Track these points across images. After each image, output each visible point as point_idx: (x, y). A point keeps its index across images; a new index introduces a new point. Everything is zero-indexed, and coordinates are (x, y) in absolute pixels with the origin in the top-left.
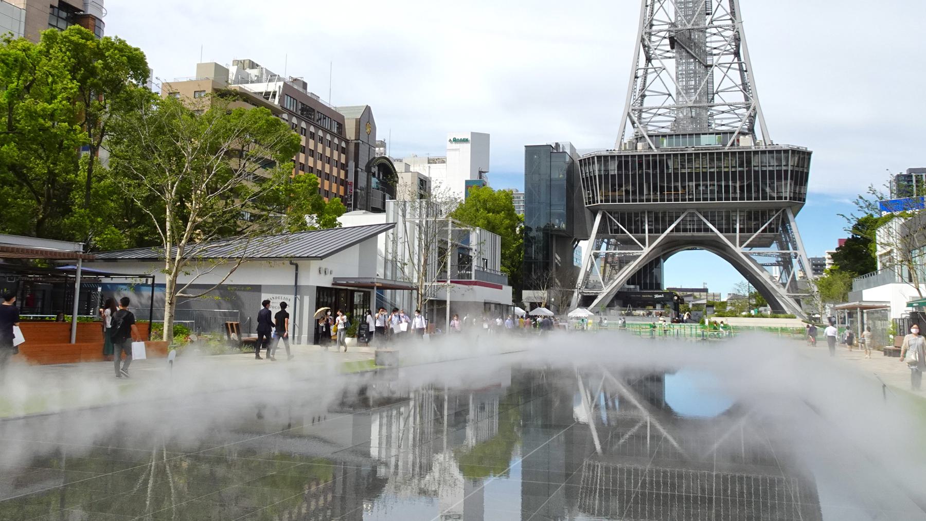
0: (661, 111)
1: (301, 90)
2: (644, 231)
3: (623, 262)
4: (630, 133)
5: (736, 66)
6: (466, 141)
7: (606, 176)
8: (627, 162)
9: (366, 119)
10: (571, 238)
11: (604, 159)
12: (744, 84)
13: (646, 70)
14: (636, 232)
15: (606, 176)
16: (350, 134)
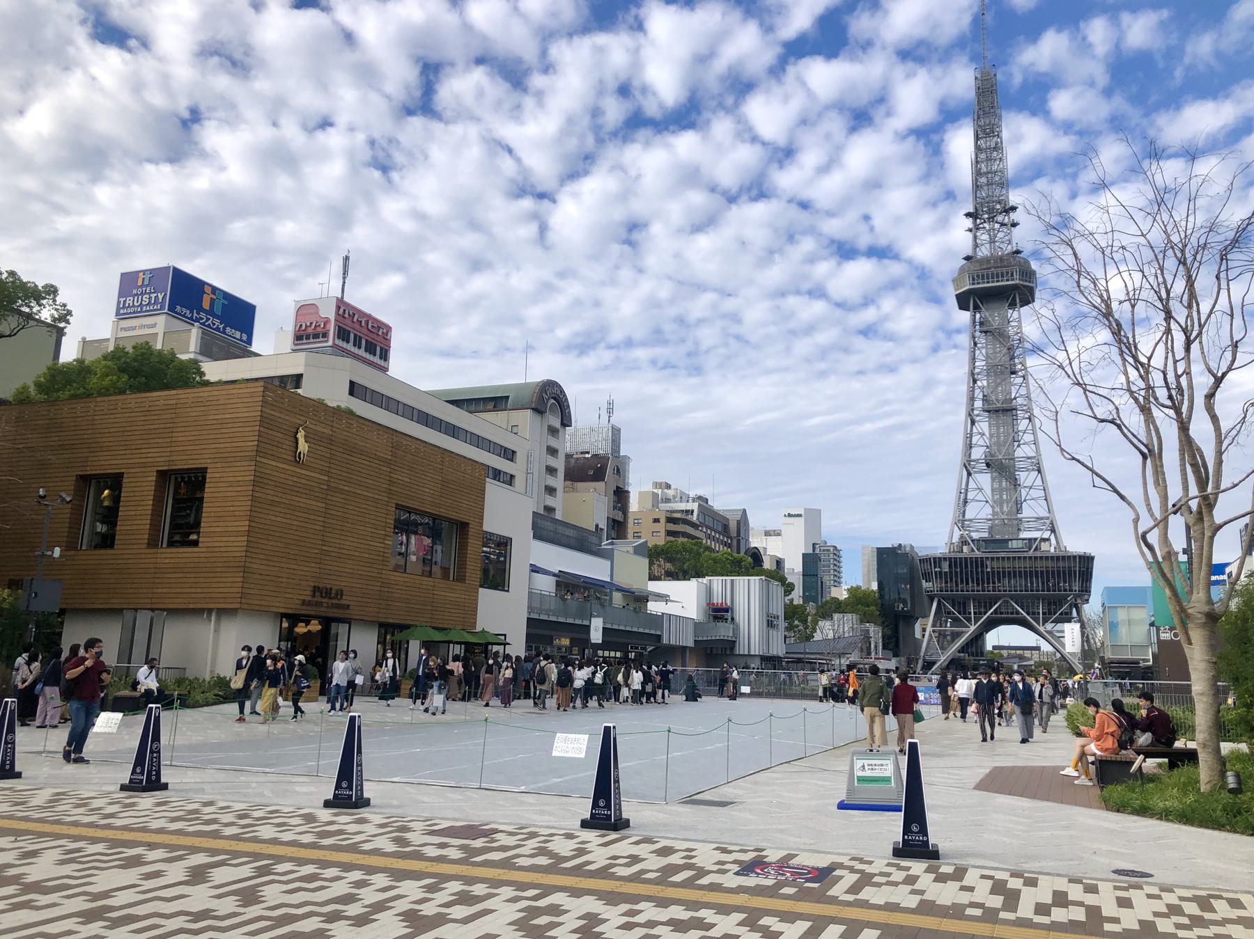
1: (705, 505)
2: (970, 613)
3: (955, 636)
6: (800, 515)
8: (955, 562)
9: (743, 522)
10: (913, 617)
11: (937, 561)
12: (1046, 496)
14: (965, 613)
16: (733, 533)
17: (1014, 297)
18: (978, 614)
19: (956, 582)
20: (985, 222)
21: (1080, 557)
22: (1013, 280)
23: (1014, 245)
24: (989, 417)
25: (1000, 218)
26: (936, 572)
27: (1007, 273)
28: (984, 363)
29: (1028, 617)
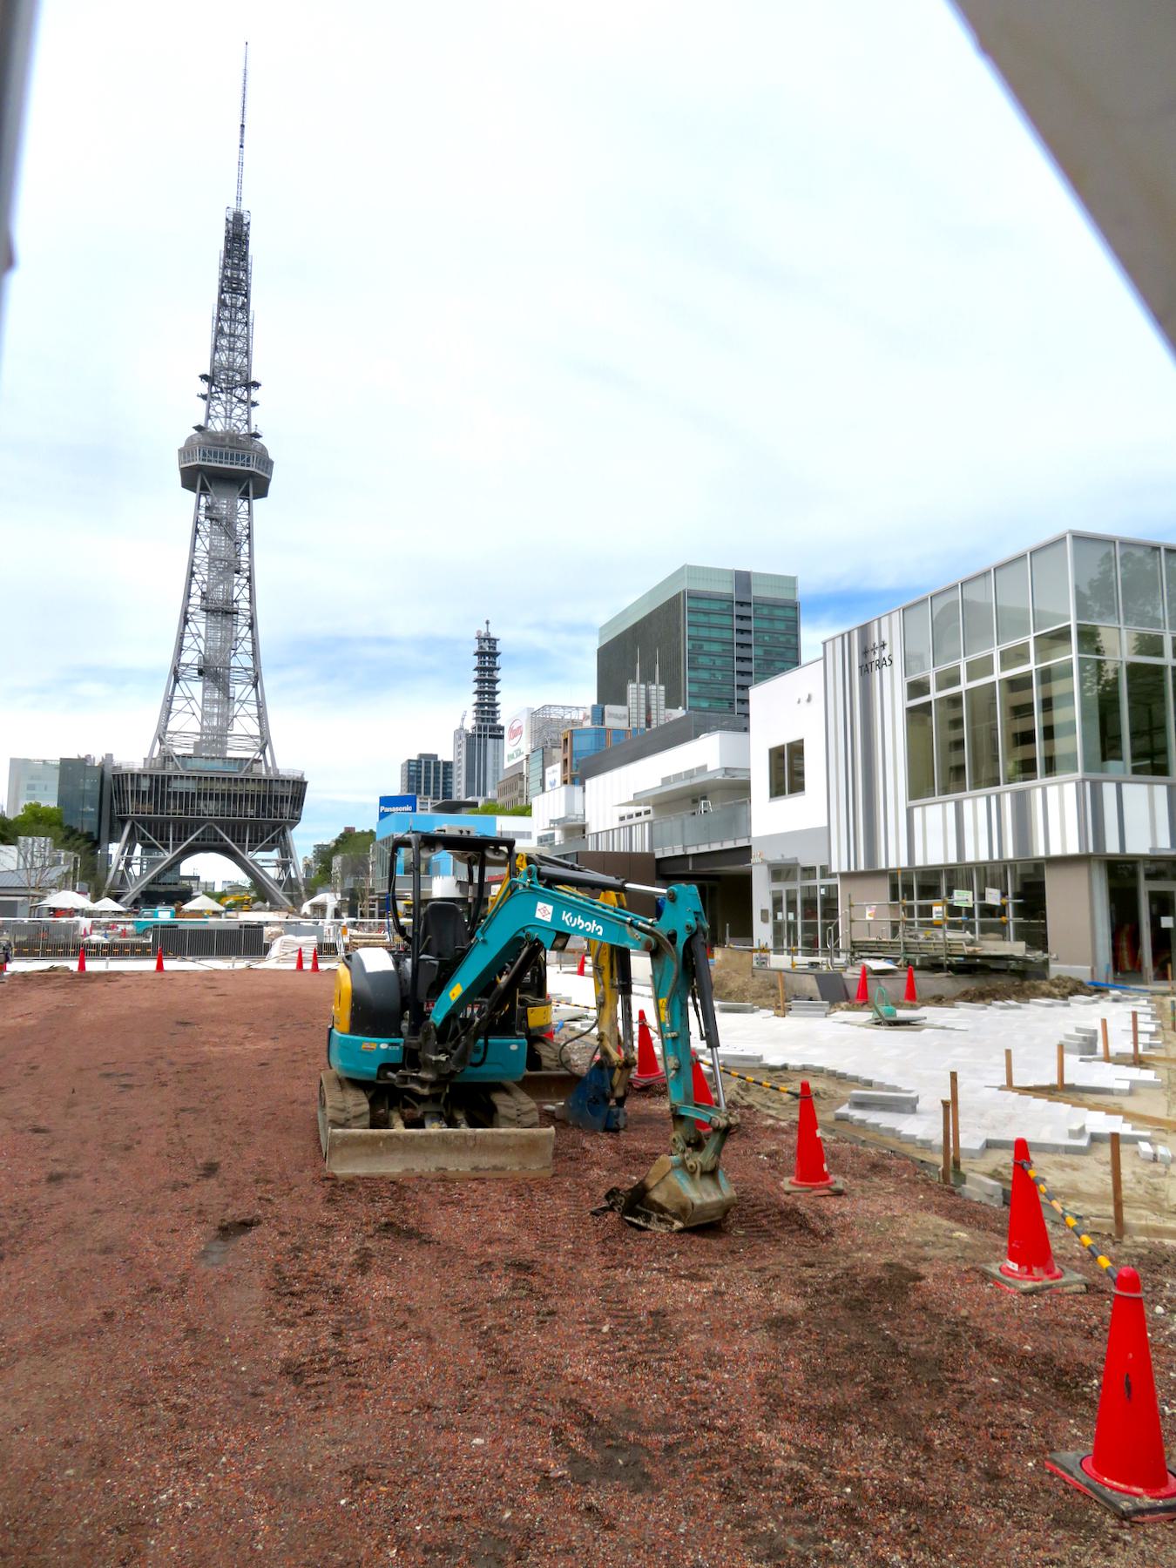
7: (138, 792)
11: (136, 777)
15: (138, 792)
17: (248, 486)
18: (179, 840)
19: (156, 802)
20: (222, 392)
22: (248, 466)
23: (253, 427)
24: (207, 618)
28: (205, 555)
29: (233, 845)
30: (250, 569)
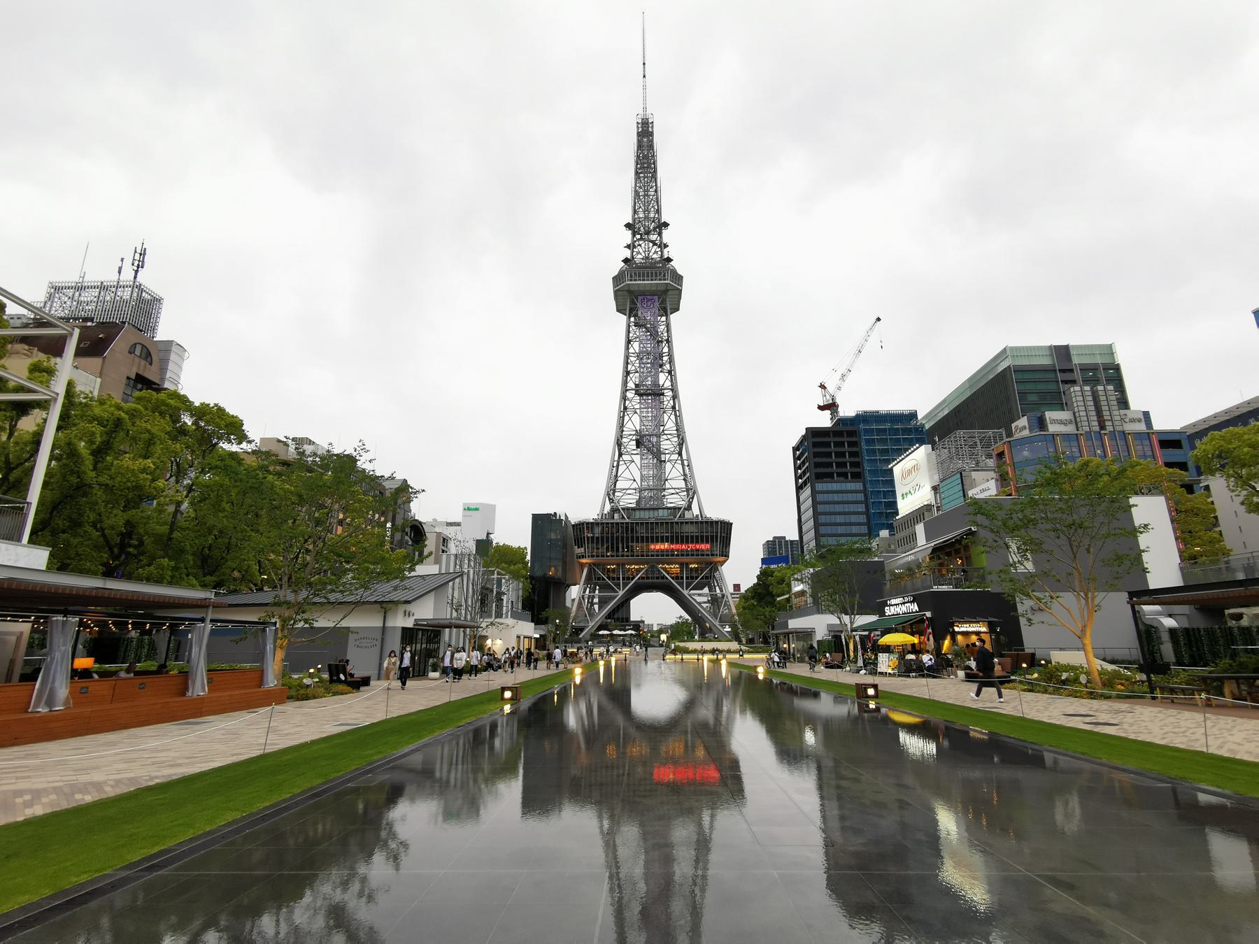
0: (629, 492)
2: (619, 579)
4: (608, 508)
5: (680, 462)
13: (618, 462)
14: (613, 579)
21: (721, 522)
22: (664, 280)
25: (654, 237)
26: (588, 538)
27: (660, 274)
29: (673, 581)
30: (671, 361)
